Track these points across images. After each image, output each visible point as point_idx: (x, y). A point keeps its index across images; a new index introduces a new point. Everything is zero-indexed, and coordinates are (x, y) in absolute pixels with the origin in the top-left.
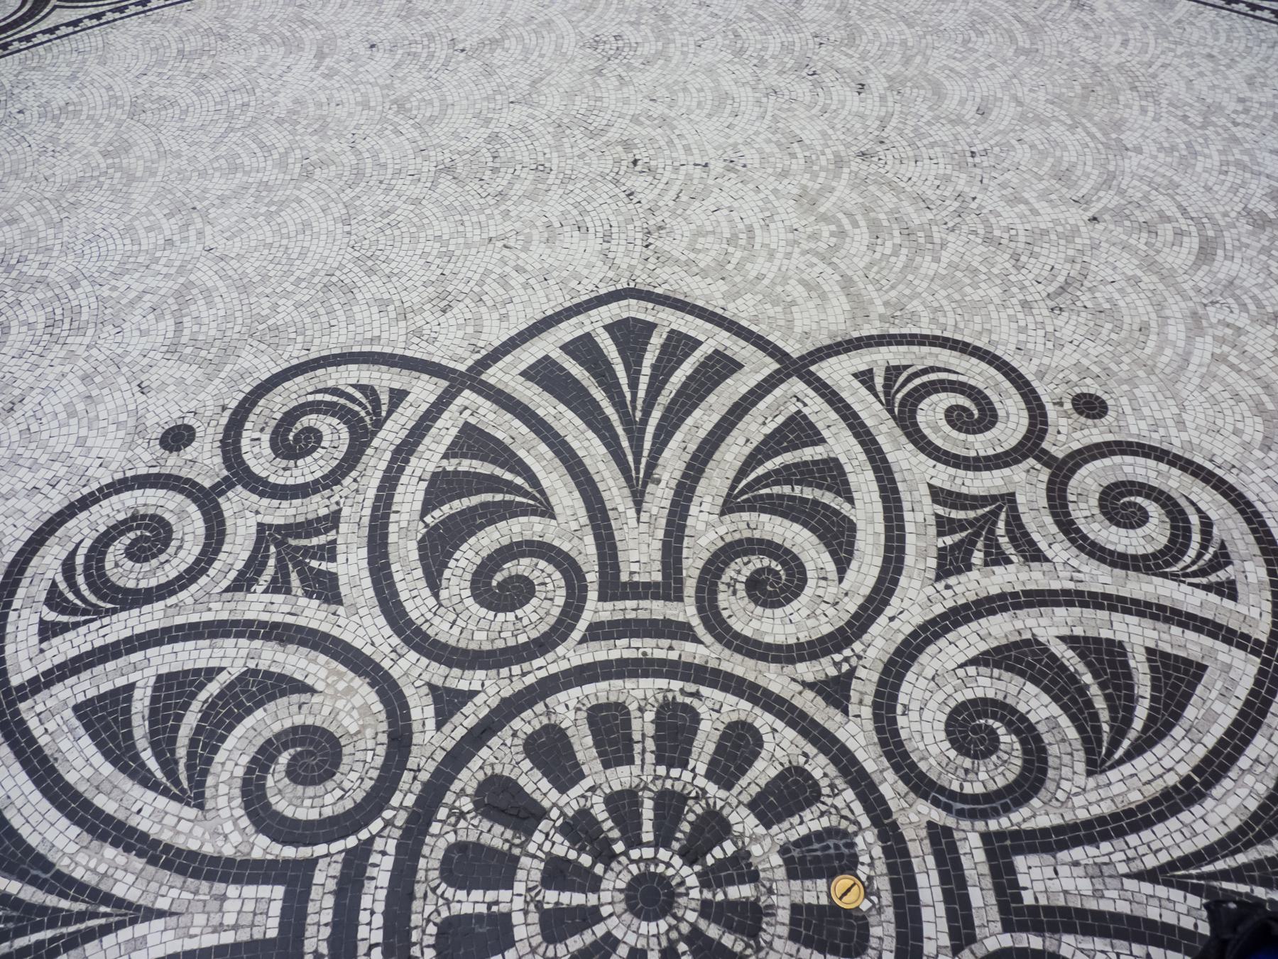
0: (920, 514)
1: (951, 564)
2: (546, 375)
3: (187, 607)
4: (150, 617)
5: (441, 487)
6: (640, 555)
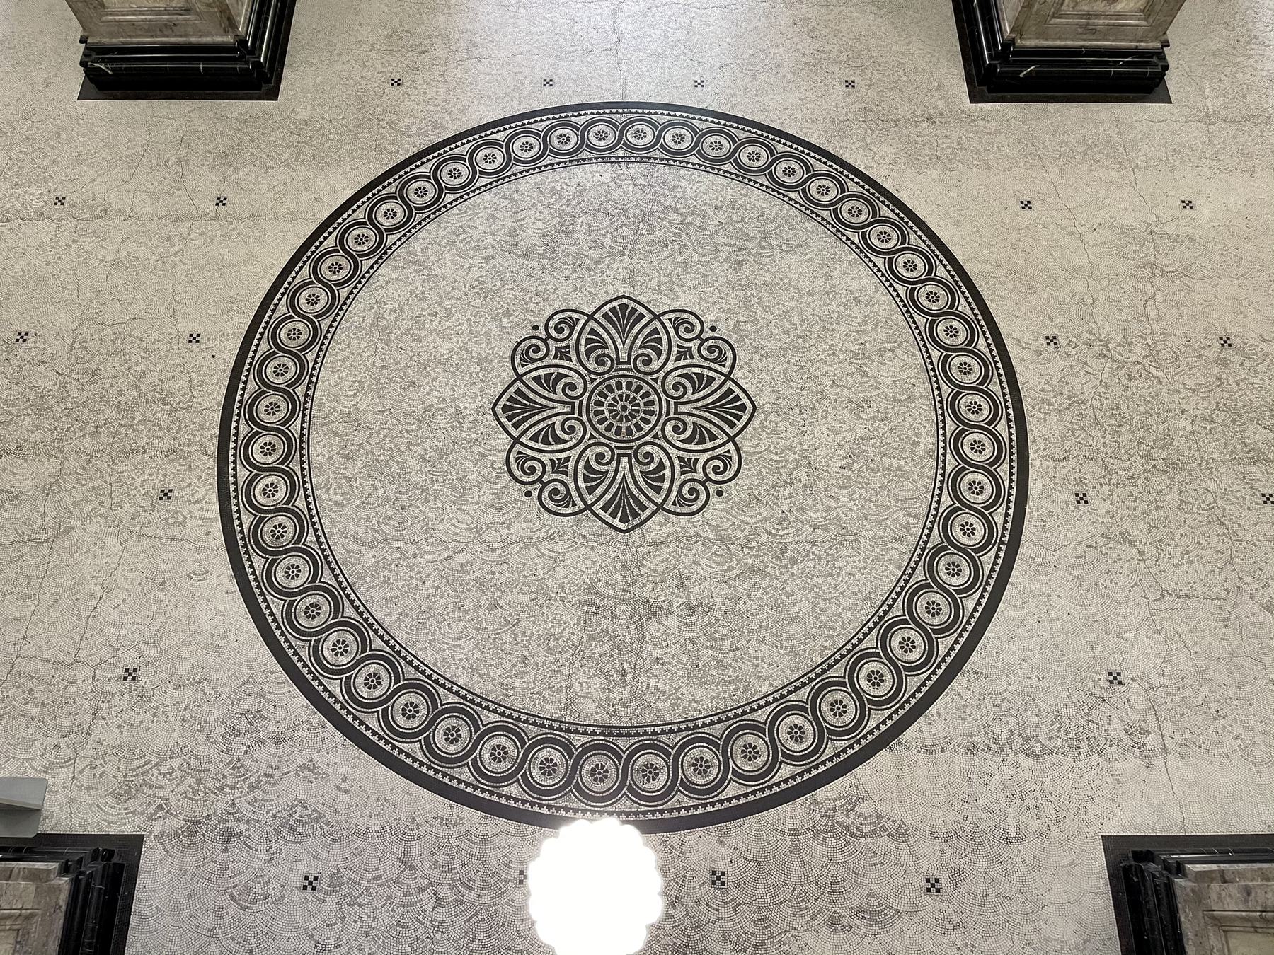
1: (677, 359)
2: (605, 316)
3: (545, 362)
4: (540, 364)
5: (588, 341)
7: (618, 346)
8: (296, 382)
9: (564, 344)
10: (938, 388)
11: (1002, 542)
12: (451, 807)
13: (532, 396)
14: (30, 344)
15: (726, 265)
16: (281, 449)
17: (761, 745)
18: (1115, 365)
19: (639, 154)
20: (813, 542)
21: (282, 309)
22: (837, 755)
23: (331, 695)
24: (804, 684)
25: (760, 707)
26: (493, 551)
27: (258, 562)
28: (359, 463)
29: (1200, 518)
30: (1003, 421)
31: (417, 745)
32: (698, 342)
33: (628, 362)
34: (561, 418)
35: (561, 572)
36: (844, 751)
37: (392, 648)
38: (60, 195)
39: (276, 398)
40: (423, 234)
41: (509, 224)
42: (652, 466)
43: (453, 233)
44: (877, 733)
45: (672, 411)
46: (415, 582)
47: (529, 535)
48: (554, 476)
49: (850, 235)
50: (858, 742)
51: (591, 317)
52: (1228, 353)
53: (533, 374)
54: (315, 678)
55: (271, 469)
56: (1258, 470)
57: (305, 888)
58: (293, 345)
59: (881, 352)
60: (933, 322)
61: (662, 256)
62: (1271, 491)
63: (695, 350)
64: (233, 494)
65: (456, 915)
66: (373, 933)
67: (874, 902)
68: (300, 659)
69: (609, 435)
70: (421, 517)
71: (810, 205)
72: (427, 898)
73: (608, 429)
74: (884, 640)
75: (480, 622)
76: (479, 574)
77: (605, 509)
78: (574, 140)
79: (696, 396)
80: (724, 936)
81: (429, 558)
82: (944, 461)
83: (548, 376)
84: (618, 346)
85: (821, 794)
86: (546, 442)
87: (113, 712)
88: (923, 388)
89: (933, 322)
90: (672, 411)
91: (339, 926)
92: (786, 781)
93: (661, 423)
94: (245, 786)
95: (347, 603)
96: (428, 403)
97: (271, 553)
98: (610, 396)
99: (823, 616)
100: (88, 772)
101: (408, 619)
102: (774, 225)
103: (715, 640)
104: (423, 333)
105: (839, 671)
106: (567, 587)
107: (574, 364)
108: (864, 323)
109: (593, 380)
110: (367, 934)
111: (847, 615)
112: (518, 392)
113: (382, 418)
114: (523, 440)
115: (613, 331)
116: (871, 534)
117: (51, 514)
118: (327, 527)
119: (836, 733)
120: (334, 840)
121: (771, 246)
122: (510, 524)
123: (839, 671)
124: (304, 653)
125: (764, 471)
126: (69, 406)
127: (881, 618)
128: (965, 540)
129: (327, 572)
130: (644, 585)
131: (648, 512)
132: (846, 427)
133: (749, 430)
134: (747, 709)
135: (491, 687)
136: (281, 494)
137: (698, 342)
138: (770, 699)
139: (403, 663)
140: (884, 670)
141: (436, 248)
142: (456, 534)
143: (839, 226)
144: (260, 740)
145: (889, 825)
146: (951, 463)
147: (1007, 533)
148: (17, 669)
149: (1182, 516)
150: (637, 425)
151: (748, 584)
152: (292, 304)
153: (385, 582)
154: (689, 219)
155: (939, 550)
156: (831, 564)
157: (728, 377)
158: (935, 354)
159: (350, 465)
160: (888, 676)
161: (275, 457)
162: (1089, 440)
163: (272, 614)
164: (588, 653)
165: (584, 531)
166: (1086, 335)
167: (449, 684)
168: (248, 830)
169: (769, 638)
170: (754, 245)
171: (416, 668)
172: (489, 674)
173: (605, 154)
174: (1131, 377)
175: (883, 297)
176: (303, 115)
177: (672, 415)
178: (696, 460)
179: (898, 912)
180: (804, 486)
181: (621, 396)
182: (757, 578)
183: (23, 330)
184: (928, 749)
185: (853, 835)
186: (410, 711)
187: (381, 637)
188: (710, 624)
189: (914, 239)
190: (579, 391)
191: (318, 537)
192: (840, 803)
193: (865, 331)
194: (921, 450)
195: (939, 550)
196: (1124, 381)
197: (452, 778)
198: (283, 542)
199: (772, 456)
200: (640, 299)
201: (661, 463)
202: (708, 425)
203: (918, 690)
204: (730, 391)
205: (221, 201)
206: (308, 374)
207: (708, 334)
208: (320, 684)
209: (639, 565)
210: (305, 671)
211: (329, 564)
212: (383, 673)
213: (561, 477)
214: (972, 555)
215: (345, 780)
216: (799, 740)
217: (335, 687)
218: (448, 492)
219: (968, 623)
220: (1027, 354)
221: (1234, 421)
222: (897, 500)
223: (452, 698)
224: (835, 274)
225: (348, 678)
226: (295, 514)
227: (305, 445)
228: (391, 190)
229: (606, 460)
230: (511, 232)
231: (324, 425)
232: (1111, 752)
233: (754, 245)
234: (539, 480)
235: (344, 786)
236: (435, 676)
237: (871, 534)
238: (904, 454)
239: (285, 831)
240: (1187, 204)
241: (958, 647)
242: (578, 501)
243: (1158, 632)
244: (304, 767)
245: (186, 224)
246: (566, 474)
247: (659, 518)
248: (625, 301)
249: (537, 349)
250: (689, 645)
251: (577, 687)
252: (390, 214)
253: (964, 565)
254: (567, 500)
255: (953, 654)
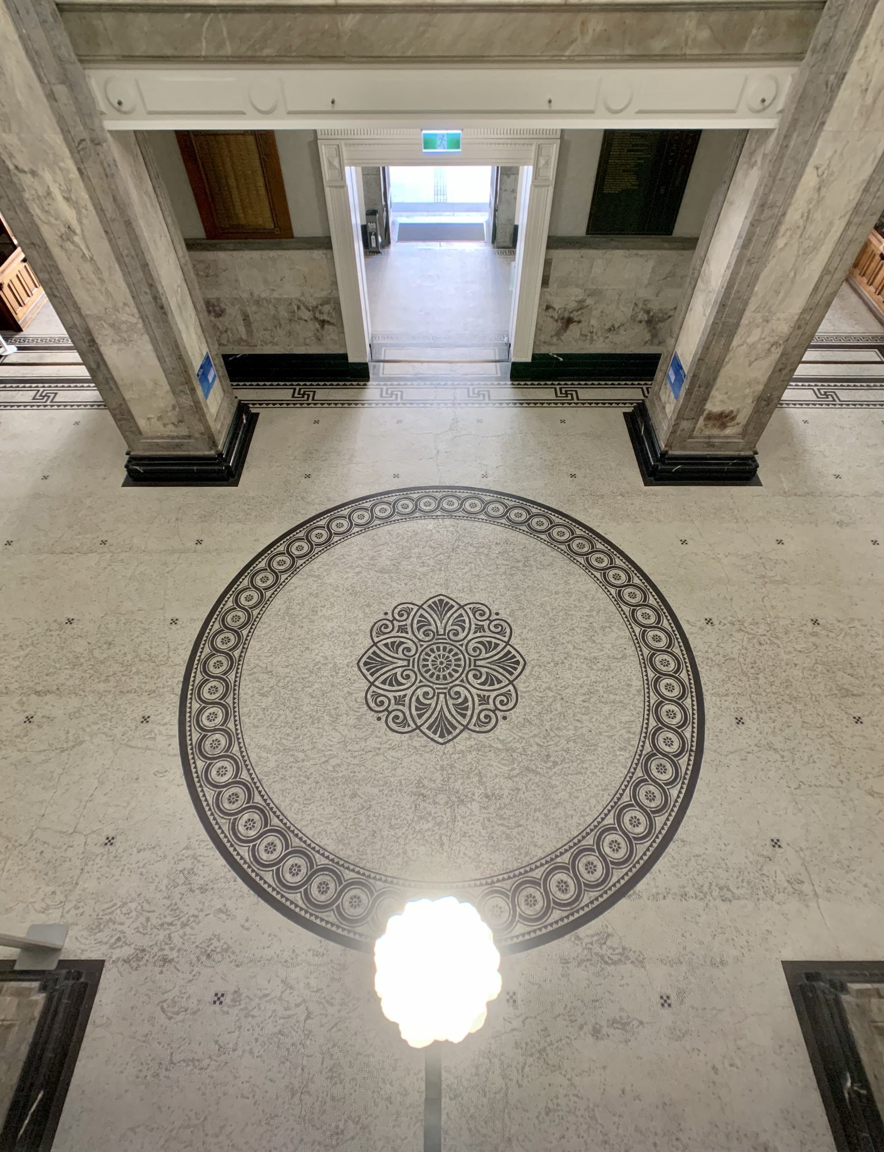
0: (473, 626)
1: (475, 632)
3: (391, 635)
4: (388, 636)
5: (419, 622)
6: (441, 631)
7: (438, 624)
8: (235, 648)
9: (404, 623)
10: (641, 651)
11: (691, 750)
12: (321, 941)
13: (383, 655)
14: (74, 625)
15: (504, 577)
16: (221, 690)
17: (538, 895)
18: (750, 636)
19: (450, 514)
20: (567, 751)
21: (230, 604)
22: (592, 902)
23: (242, 858)
24: (566, 851)
25: (537, 867)
26: (355, 757)
27: (201, 764)
28: (270, 699)
29: (816, 733)
30: (684, 671)
31: (299, 895)
32: (488, 622)
33: (444, 634)
34: (401, 669)
35: (399, 771)
36: (597, 899)
37: (285, 824)
38: (104, 539)
39: (221, 658)
40: (319, 559)
41: (371, 553)
42: (460, 700)
43: (337, 558)
44: (618, 886)
45: (473, 664)
46: (302, 778)
47: (379, 746)
48: (396, 707)
49: (578, 559)
50: (606, 892)
51: (420, 607)
52: (817, 629)
53: (384, 642)
54: (232, 845)
55: (213, 703)
56: (849, 701)
57: (215, 1002)
58: (235, 625)
59: (603, 628)
60: (634, 610)
61: (464, 571)
62: (859, 715)
63: (486, 627)
64: (188, 719)
65: (322, 1026)
66: (261, 1039)
67: (624, 1015)
68: (223, 832)
69: (431, 680)
70: (309, 735)
71: (553, 542)
72: (301, 1013)
73: (432, 676)
74: (619, 818)
75: (345, 807)
76: (345, 773)
77: (429, 728)
78: (411, 506)
79: (488, 655)
80: (516, 1043)
81: (312, 762)
82: (649, 697)
83: (393, 643)
84: (438, 624)
85: (582, 931)
86: (391, 684)
87: (96, 867)
88: (631, 650)
89: (634, 610)
90: (473, 664)
91: (237, 1033)
92: (556, 922)
93: (465, 672)
94: (179, 923)
95: (256, 793)
96: (317, 660)
97: (209, 759)
98: (433, 655)
99: (577, 802)
100: (73, 912)
101: (296, 805)
102: (532, 553)
103: (504, 819)
104: (316, 618)
105: (589, 841)
106: (403, 782)
107: (410, 635)
108: (591, 611)
109: (421, 646)
110: (257, 1040)
111: (593, 801)
112: (374, 653)
113: (287, 670)
114: (376, 683)
115: (434, 616)
116: (605, 745)
117: (72, 731)
118: (247, 741)
119: (590, 886)
120: (237, 966)
121: (531, 566)
122: (366, 740)
123: (589, 841)
124: (225, 828)
125: (533, 703)
126: (92, 663)
127: (616, 803)
128: (667, 749)
129: (245, 772)
130: (456, 781)
131: (458, 731)
132: (584, 675)
133: (522, 676)
134: (528, 869)
135: (351, 853)
136: (219, 719)
137: (488, 622)
138: (543, 861)
139: (291, 835)
140: (620, 840)
141: (326, 567)
142: (331, 746)
143: (572, 554)
144: (192, 891)
145: (631, 954)
146: (654, 698)
147: (694, 744)
148: (35, 837)
149: (804, 732)
150: (450, 674)
151: (526, 779)
152: (236, 601)
153: (282, 778)
154: (481, 550)
155: (651, 756)
156: (580, 766)
157: (507, 643)
158: (637, 630)
159: (264, 699)
160: (623, 845)
161: (217, 695)
162: (740, 683)
163: (206, 800)
164: (418, 828)
165: (415, 744)
166: (730, 618)
167: (322, 851)
168: (178, 957)
169: (541, 817)
170: (520, 564)
171: (301, 839)
172: (349, 844)
173: (430, 514)
174: (761, 644)
175: (601, 595)
176: (252, 494)
177: (472, 667)
178: (489, 697)
179: (641, 1023)
180: (560, 713)
181: (439, 655)
182: (531, 775)
183: (71, 617)
184: (655, 897)
185: (606, 963)
186: (295, 870)
187: (278, 817)
188: (500, 808)
189: (618, 562)
190: (413, 652)
191: (240, 748)
192: (595, 938)
193: (592, 616)
194: (633, 690)
195: (651, 756)
196: (757, 646)
197: (322, 920)
198: (217, 751)
199: (538, 694)
200: (451, 596)
201: (466, 698)
202: (495, 673)
203: (645, 854)
204: (509, 652)
205: (199, 542)
206: (242, 642)
207: (494, 617)
208: (235, 850)
209: (452, 767)
210: (225, 840)
211: (247, 766)
212: (277, 842)
213: (400, 707)
214: (673, 759)
215: (247, 920)
216: (565, 891)
217: (244, 851)
218: (327, 718)
219: (674, 806)
220: (694, 630)
221: (828, 671)
222: (621, 723)
223: (325, 861)
224: (571, 582)
225: (254, 846)
226: (227, 732)
227: (237, 688)
228: (301, 535)
229: (430, 696)
230: (373, 558)
231: (250, 675)
232: (779, 897)
233: (520, 564)
234: (386, 709)
235: (247, 925)
236: (313, 845)
237: (605, 745)
238: (623, 693)
239: (203, 958)
240: (780, 542)
241: (669, 823)
242: (411, 723)
243: (800, 810)
244: (220, 911)
245: (176, 555)
246: (404, 705)
247: (465, 734)
248: (442, 597)
249: (387, 627)
250: (487, 823)
251: (410, 853)
252: (300, 548)
253: (668, 766)
254: (404, 723)
255: (666, 828)
